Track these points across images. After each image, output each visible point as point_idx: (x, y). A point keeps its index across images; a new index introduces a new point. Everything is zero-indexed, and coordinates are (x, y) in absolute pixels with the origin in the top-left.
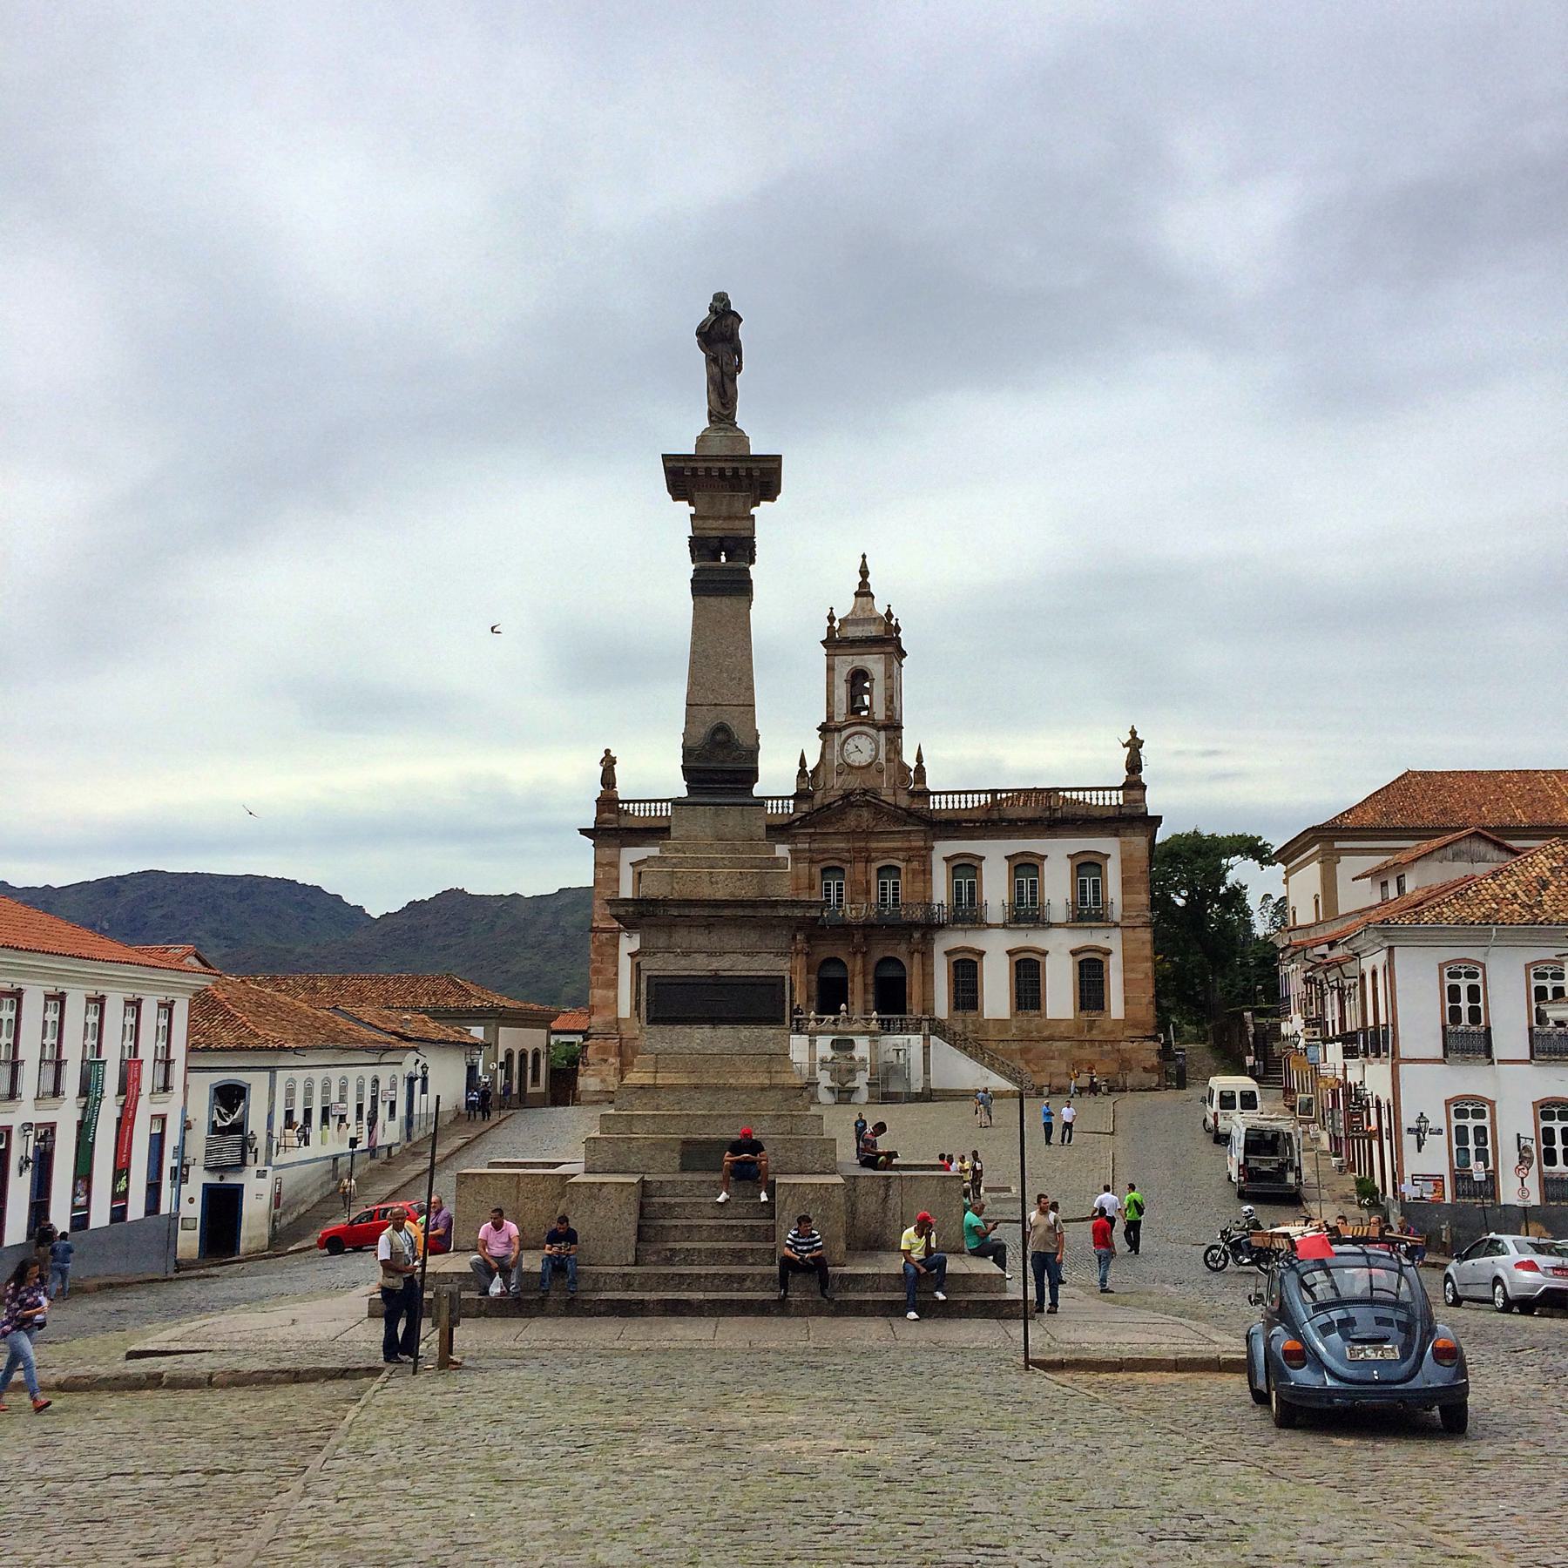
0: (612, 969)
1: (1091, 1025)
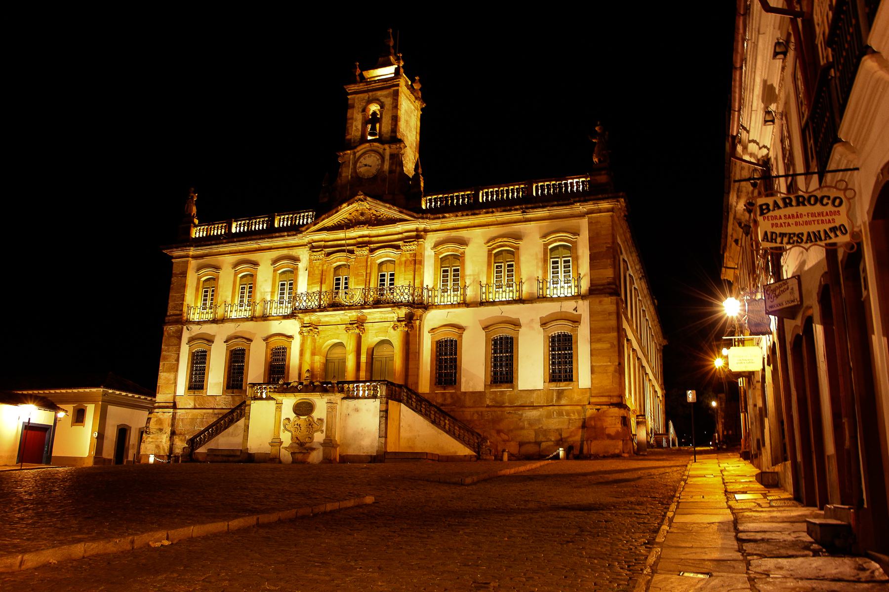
0: (174, 356)
1: (560, 393)
